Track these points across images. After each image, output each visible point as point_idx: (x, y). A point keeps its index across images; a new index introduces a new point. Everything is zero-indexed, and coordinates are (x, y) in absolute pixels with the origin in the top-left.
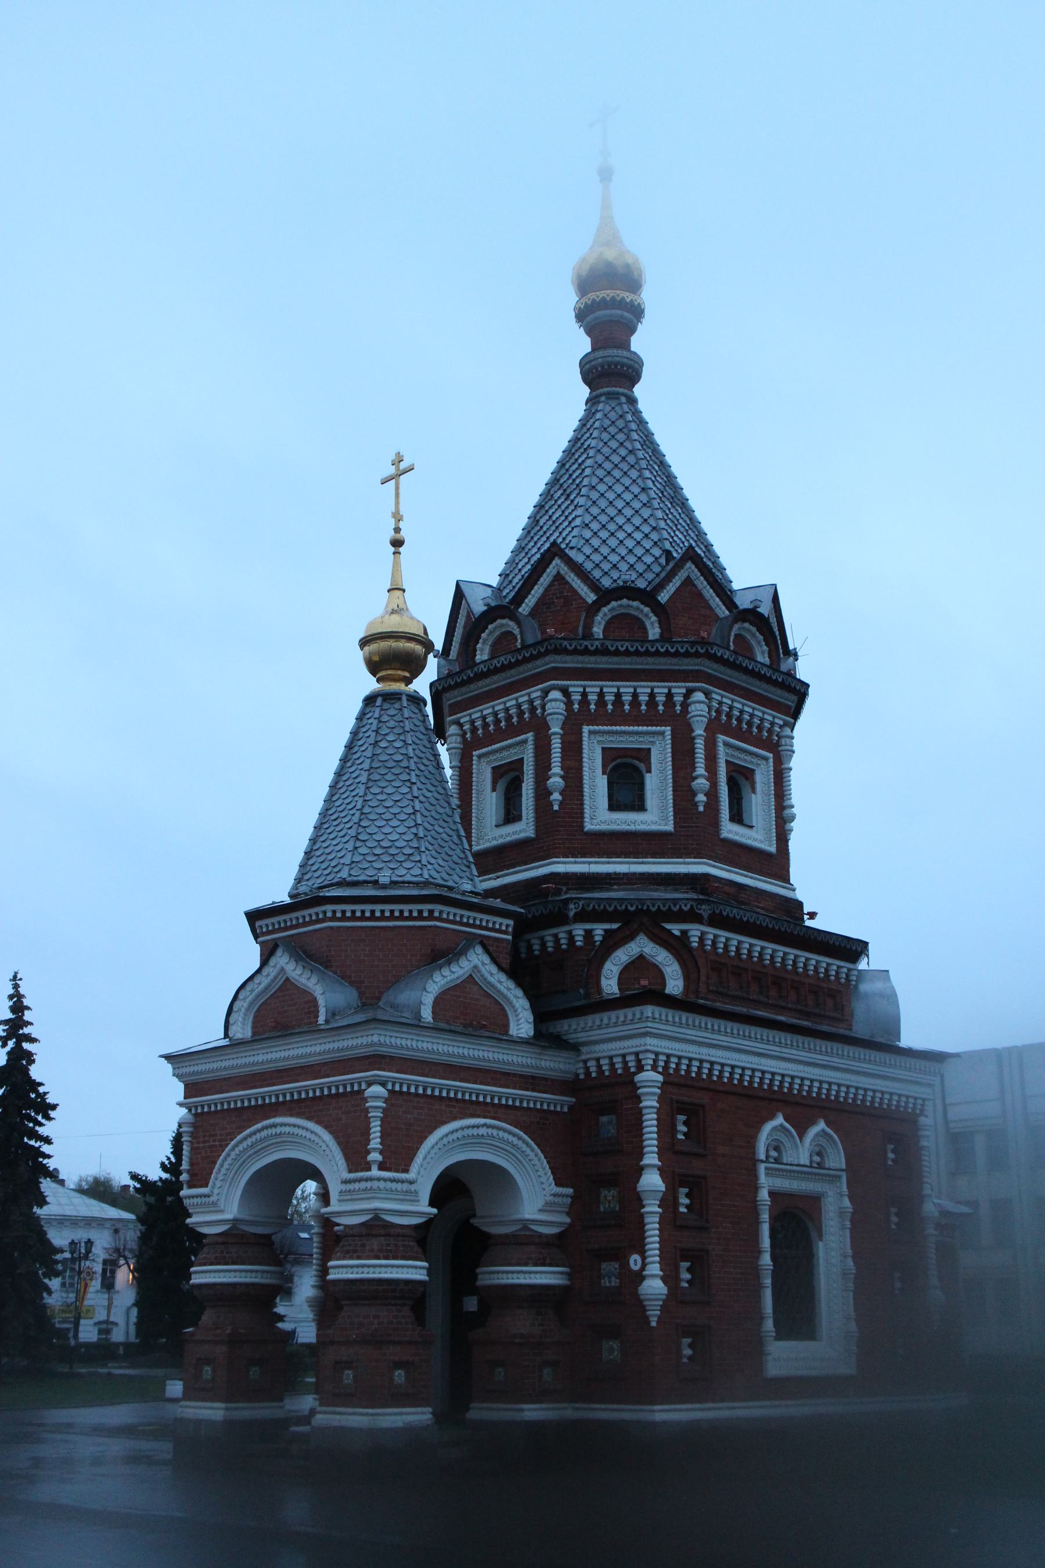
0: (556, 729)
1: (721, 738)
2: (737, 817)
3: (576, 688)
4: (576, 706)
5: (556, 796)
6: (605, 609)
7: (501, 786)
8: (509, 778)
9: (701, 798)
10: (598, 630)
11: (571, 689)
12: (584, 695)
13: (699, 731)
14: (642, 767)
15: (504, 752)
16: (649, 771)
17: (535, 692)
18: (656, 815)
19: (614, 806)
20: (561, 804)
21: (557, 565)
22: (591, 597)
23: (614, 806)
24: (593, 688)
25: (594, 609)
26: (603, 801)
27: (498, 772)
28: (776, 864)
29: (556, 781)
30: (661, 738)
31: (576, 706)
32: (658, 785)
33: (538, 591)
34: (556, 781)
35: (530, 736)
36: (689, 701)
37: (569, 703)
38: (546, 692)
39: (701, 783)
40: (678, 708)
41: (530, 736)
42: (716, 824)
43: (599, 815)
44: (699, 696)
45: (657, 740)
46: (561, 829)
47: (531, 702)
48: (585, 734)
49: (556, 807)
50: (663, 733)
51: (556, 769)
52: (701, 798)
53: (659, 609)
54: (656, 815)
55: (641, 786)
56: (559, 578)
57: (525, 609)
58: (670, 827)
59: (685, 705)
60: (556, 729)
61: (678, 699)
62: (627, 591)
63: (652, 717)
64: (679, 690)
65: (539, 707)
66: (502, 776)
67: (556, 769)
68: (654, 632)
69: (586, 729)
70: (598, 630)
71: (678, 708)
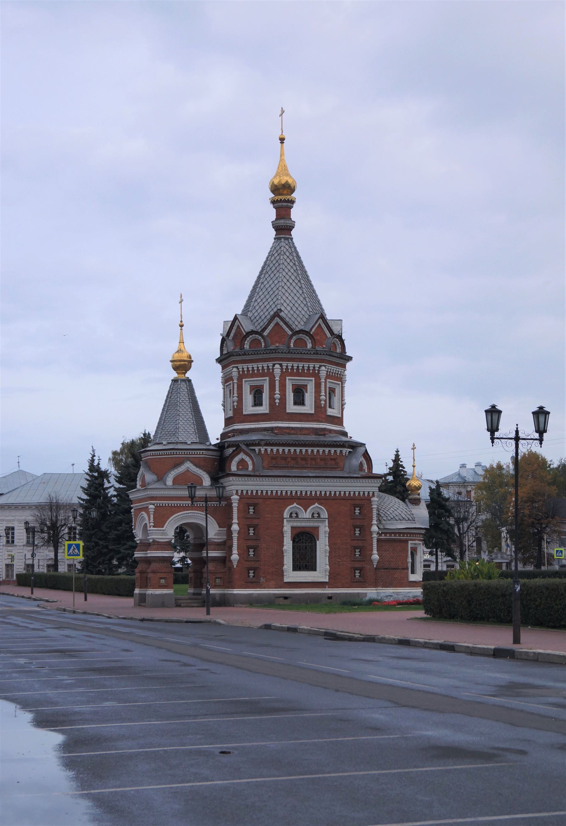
0: (277, 378)
1: (328, 380)
2: (330, 407)
3: (284, 364)
4: (284, 370)
5: (277, 401)
6: (294, 337)
7: (253, 393)
8: (257, 393)
9: (323, 402)
10: (292, 345)
12: (287, 366)
14: (304, 390)
15: (257, 381)
18: (308, 408)
19: (295, 403)
20: (279, 403)
21: (277, 319)
22: (290, 333)
23: (295, 403)
24: (290, 364)
25: (291, 337)
28: (339, 421)
29: (277, 396)
31: (284, 370)
32: (309, 397)
33: (270, 328)
34: (277, 396)
35: (267, 378)
37: (282, 369)
38: (274, 365)
41: (267, 378)
42: (326, 411)
43: (291, 408)
44: (323, 368)
45: (310, 382)
46: (279, 411)
47: (268, 367)
48: (287, 380)
49: (277, 404)
50: (312, 380)
51: (277, 391)
52: (323, 402)
53: (311, 337)
54: (308, 408)
55: (303, 396)
56: (277, 324)
57: (265, 333)
58: (313, 412)
59: (319, 371)
60: (277, 378)
62: (301, 331)
64: (317, 365)
67: (277, 391)
68: (309, 346)
70: (292, 345)
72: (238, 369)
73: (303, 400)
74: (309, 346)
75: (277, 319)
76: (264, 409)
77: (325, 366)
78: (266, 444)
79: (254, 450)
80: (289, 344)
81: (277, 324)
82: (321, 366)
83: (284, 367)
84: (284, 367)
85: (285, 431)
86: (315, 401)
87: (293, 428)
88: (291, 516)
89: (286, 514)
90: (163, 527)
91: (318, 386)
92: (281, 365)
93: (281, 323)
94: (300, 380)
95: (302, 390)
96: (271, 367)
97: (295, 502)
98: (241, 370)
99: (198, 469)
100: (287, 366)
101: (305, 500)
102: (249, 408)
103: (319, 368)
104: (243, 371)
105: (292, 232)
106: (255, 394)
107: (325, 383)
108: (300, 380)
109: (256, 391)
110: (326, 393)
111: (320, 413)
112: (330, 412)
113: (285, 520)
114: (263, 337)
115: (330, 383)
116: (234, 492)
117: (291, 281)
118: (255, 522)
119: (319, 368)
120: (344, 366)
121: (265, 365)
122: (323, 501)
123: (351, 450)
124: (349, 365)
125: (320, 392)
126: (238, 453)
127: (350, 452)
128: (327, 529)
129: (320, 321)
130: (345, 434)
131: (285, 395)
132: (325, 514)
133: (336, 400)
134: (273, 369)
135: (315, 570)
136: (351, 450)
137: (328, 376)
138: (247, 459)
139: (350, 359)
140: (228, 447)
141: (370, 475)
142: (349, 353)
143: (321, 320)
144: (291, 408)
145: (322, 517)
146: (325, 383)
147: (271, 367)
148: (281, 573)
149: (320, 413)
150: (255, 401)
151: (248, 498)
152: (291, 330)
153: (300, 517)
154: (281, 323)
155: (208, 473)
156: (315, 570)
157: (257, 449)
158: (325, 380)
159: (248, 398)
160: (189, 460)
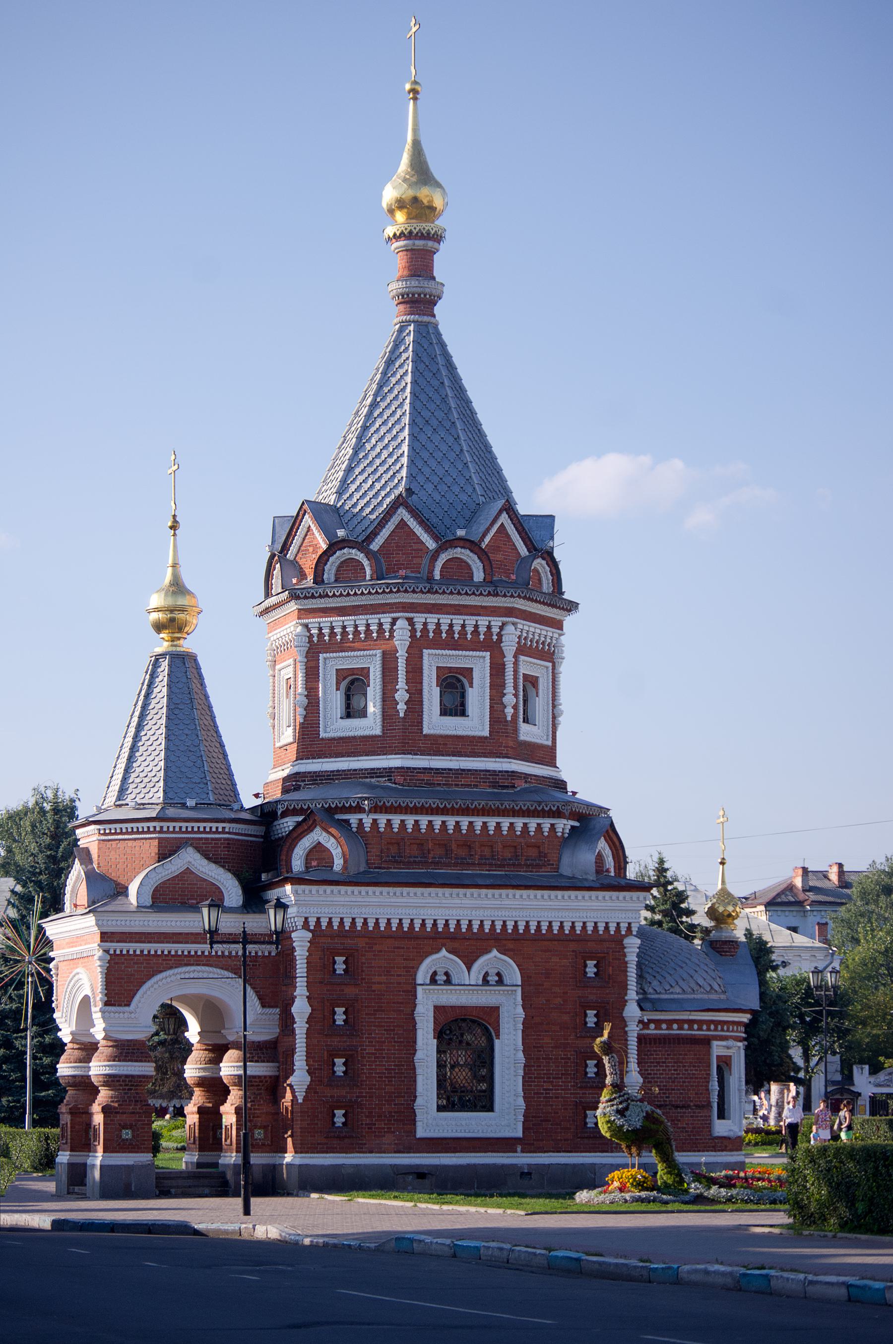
1: (522, 658)
2: (526, 720)
3: (419, 619)
4: (419, 634)
7: (344, 685)
11: (415, 620)
12: (425, 624)
13: (509, 659)
15: (351, 661)
16: (471, 686)
17: (386, 619)
18: (476, 722)
19: (444, 712)
22: (431, 544)
23: (444, 712)
24: (432, 619)
26: (437, 709)
27: (341, 674)
28: (546, 755)
30: (482, 660)
32: (478, 697)
33: (385, 533)
36: (503, 633)
37: (413, 631)
38: (394, 621)
39: (509, 699)
40: (495, 638)
42: (516, 730)
43: (434, 722)
44: (510, 629)
47: (380, 625)
49: (402, 715)
51: (402, 684)
52: (509, 711)
53: (482, 555)
55: (463, 695)
57: (375, 546)
58: (486, 733)
59: (500, 635)
61: (495, 630)
63: (476, 645)
64: (496, 622)
65: (387, 630)
66: (345, 678)
67: (402, 684)
68: (479, 575)
69: (426, 652)
71: (495, 638)
72: (309, 630)
73: (463, 704)
74: (479, 575)
75: (402, 513)
76: (370, 724)
77: (514, 624)
78: (375, 809)
79: (347, 821)
80: (431, 571)
81: (402, 524)
82: (504, 624)
83: (419, 627)
84: (419, 627)
85: (422, 776)
86: (491, 707)
87: (438, 771)
88: (433, 981)
89: (422, 975)
90: (129, 1005)
91: (497, 670)
92: (410, 621)
93: (412, 523)
94: (455, 659)
95: (459, 681)
96: (387, 627)
97: (444, 945)
98: (315, 631)
99: (213, 866)
100: (425, 624)
101: (469, 943)
102: (334, 725)
103: (501, 628)
104: (321, 634)
105: (437, 310)
106: (348, 689)
107: (516, 664)
108: (455, 659)
109: (352, 682)
110: (516, 687)
111: (502, 737)
112: (527, 733)
113: (419, 989)
114: (369, 554)
115: (529, 666)
116: (300, 922)
117: (435, 423)
118: (350, 991)
119: (501, 628)
120: (558, 625)
121: (373, 620)
122: (510, 945)
123: (577, 824)
124: (570, 622)
125: (503, 685)
126: (310, 830)
127: (573, 827)
128: (520, 1010)
129: (504, 518)
130: (561, 785)
131: (420, 692)
132: (514, 975)
133: (540, 704)
134: (392, 631)
135: (490, 1108)
136: (577, 824)
137: (522, 650)
138: (330, 843)
139: (571, 607)
140: (285, 814)
141: (623, 882)
142: (570, 592)
143: (504, 515)
144: (434, 722)
145: (507, 980)
146: (516, 664)
147: (387, 627)
148: (411, 1118)
149: (502, 737)
150: (348, 706)
151: (332, 937)
152: (436, 538)
153: (455, 980)
154: (412, 523)
155: (237, 875)
156: (490, 1108)
157: (353, 819)
158: (515, 657)
159: (332, 699)
160: (191, 845)
